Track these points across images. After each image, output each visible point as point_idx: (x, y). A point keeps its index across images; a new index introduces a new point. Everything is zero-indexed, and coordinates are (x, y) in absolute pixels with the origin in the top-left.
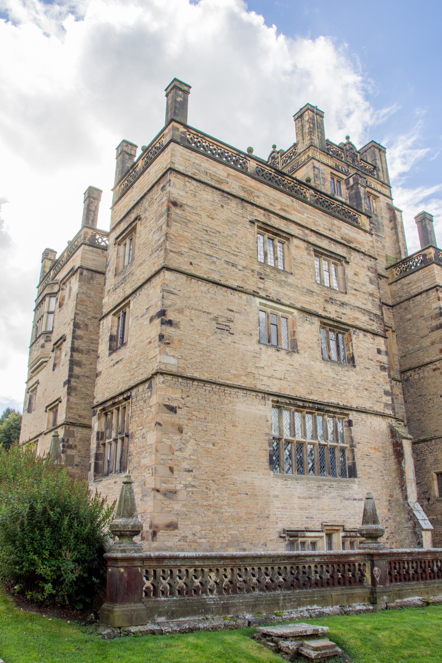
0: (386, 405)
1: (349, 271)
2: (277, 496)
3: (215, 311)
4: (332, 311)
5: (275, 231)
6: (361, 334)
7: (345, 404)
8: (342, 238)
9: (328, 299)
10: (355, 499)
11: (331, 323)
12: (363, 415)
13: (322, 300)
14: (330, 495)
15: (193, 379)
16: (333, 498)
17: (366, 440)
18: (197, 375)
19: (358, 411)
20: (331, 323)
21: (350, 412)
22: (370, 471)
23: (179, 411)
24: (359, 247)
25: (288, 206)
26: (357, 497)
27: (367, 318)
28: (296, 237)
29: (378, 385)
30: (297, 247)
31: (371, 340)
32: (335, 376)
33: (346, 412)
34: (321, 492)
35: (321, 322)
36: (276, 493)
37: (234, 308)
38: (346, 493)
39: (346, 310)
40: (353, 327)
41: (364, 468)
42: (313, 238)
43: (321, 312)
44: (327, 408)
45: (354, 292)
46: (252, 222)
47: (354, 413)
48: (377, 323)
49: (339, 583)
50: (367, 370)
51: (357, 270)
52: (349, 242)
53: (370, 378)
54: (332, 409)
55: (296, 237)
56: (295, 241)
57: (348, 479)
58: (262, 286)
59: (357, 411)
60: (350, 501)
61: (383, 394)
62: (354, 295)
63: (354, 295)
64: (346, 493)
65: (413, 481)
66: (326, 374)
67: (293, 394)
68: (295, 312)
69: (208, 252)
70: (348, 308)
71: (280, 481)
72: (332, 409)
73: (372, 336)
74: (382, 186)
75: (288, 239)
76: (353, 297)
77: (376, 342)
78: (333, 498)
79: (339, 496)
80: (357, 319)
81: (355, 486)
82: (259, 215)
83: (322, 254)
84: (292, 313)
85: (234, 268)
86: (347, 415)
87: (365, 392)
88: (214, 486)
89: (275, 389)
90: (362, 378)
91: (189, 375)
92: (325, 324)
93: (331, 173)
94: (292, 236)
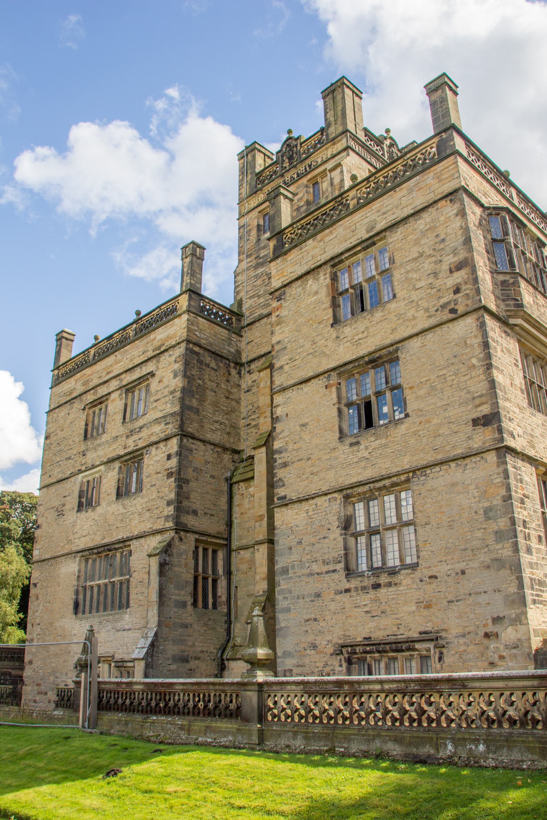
0: (167, 518)
1: (154, 384)
2: (75, 635)
3: (57, 504)
4: (131, 445)
5: (99, 401)
6: (153, 449)
7: (128, 535)
8: (153, 351)
9: (129, 434)
10: (124, 630)
11: (128, 457)
12: (142, 540)
13: (124, 438)
14: (107, 629)
15: (44, 561)
16: (108, 631)
17: (142, 566)
18: (47, 556)
19: (138, 538)
20: (128, 457)
21: (131, 543)
22: (142, 598)
23: (38, 585)
24: (167, 344)
25: (111, 365)
26: (127, 627)
27: (163, 425)
28: (113, 392)
29: (162, 498)
30: (113, 401)
31: (164, 448)
32: (124, 511)
33: (127, 543)
34: (101, 627)
35: (122, 462)
36: (75, 632)
37: (67, 494)
38: (119, 625)
39: (145, 433)
40: (145, 447)
41: (136, 596)
42: (128, 378)
43: (122, 453)
44: (114, 547)
45: (155, 404)
46: (84, 409)
47: (134, 541)
48: (173, 423)
49: (142, 712)
50: (152, 488)
51: (162, 375)
52: (160, 347)
53: (155, 495)
54: (117, 546)
55: (113, 392)
56: (113, 396)
57: (109, 612)
58: (83, 461)
59: (136, 538)
60: (121, 632)
61: (165, 506)
62: (153, 409)
63: (153, 409)
64: (119, 625)
65: (155, 603)
66: (118, 513)
67: (91, 545)
68: (102, 468)
69: (58, 459)
70: (145, 429)
71: (78, 622)
72: (117, 546)
73: (164, 443)
74: (334, 144)
75: (107, 399)
76: (152, 412)
77: (169, 447)
78: (108, 631)
79: (113, 628)
80: (152, 434)
81: (127, 617)
82: (90, 397)
83: (134, 387)
84: (100, 471)
85: (70, 461)
86: (130, 546)
87: (148, 514)
88: (48, 633)
89: (82, 547)
90: (146, 500)
91: (43, 558)
92: (126, 461)
93: (260, 212)
94: (109, 394)
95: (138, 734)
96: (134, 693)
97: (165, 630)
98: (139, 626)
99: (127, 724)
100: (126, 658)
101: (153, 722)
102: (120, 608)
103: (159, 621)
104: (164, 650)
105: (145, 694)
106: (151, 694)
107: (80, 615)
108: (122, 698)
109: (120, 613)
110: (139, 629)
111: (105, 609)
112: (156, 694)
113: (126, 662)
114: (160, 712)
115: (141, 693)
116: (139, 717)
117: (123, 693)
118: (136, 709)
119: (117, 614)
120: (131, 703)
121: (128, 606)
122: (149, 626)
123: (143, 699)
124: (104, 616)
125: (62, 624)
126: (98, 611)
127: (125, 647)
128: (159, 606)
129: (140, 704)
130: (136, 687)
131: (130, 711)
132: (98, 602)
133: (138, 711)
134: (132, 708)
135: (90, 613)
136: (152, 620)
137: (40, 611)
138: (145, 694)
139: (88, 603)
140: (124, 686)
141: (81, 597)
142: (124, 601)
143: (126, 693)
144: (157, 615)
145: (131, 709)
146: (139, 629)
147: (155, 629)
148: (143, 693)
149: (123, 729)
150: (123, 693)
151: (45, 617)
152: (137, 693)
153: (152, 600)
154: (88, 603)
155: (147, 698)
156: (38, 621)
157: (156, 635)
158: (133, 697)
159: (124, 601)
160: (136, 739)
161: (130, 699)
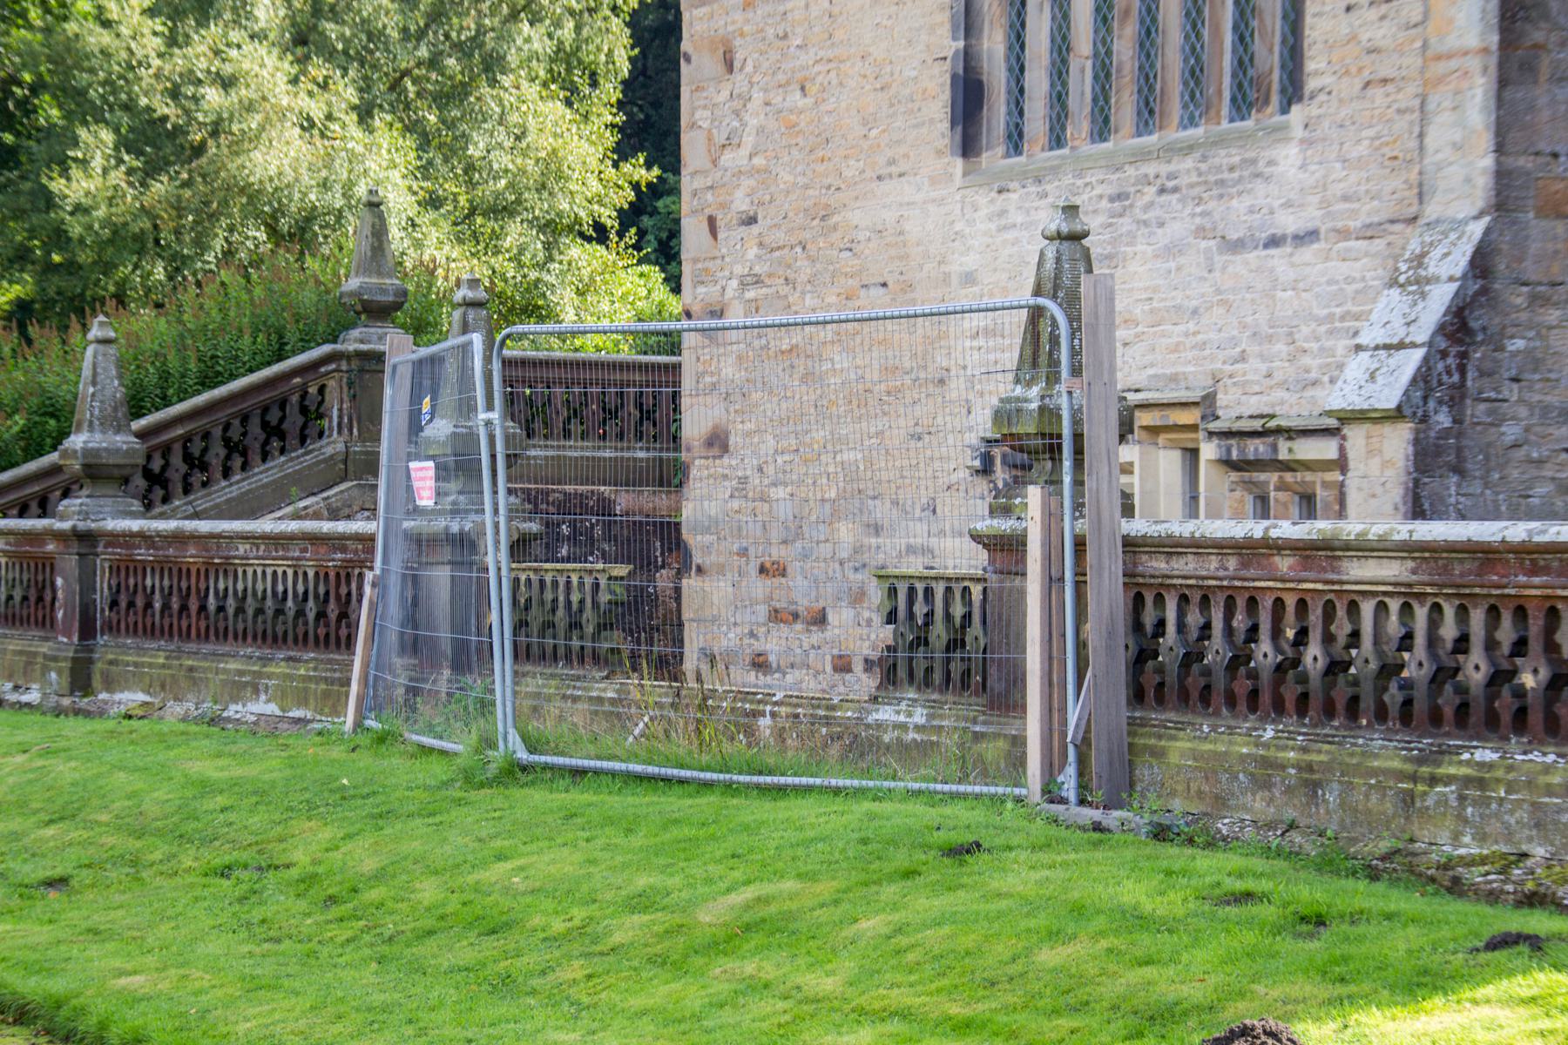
10: (1274, 242)
14: (1163, 237)
16: (1172, 250)
26: (1289, 223)
34: (1125, 224)
36: (970, 261)
38: (1237, 213)
41: (1344, 26)
57: (1174, 134)
60: (1252, 257)
64: (1237, 213)
65: (1474, 64)
71: (984, 199)
78: (1172, 250)
79: (1200, 232)
81: (1288, 158)
88: (804, 270)
95: (1384, 846)
96: (1353, 608)
97: (1541, 233)
98: (1368, 211)
99: (1311, 783)
100: (1292, 409)
101: (1479, 781)
102: (1242, 104)
103: (1502, 176)
104: (1534, 361)
105: (1421, 613)
106: (1462, 612)
107: (993, 157)
108: (1277, 633)
109: (1244, 138)
110: (1369, 233)
111: (1148, 114)
112: (1493, 612)
113: (1291, 433)
114: (1520, 720)
115: (1394, 605)
116: (1385, 751)
117: (1279, 603)
118: (1368, 702)
119: (1220, 141)
120: (1336, 667)
121: (1293, 91)
122: (1432, 211)
123: (1406, 641)
124: (1142, 156)
125: (889, 216)
126: (1102, 128)
127: (1281, 348)
128: (1503, 83)
129: (1389, 670)
130: (1360, 571)
131: (1329, 711)
132: (1103, 73)
133: (1381, 714)
134: (1341, 693)
135: (1057, 139)
136: (1455, 173)
137: (749, 140)
138: (1421, 613)
139: (1038, 81)
140: (1284, 564)
141: (994, 44)
142: (1269, 57)
143: (1302, 605)
144: (1486, 141)
145: (1335, 700)
146: (1369, 233)
147: (1477, 229)
148: (1406, 609)
149: (1290, 814)
150: (1279, 603)
151: (786, 177)
152: (1367, 608)
153: (1452, 42)
154: (1038, 81)
155: (1433, 641)
156: (741, 204)
157: (1481, 263)
158: (1342, 628)
159: (1269, 57)
160: (1373, 875)
161: (1328, 639)
